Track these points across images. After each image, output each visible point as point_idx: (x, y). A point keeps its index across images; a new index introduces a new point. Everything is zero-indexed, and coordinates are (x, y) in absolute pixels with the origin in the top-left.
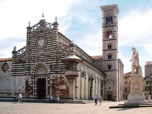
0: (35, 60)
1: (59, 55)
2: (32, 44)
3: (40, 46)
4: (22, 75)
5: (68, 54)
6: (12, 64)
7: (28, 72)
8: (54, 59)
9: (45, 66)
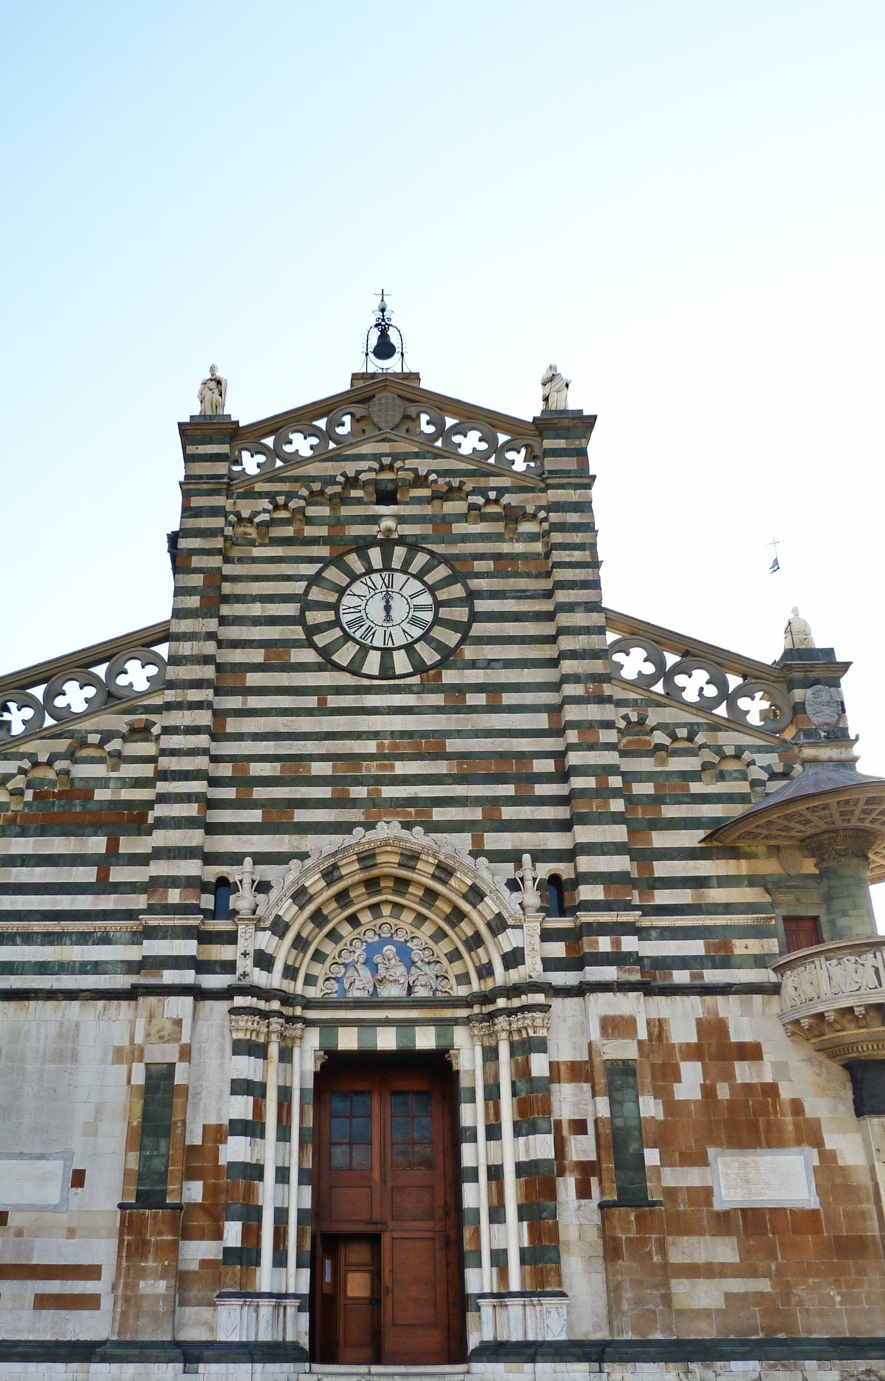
0: (303, 804)
2: (257, 609)
3: (364, 650)
7: (188, 947)
9: (461, 881)
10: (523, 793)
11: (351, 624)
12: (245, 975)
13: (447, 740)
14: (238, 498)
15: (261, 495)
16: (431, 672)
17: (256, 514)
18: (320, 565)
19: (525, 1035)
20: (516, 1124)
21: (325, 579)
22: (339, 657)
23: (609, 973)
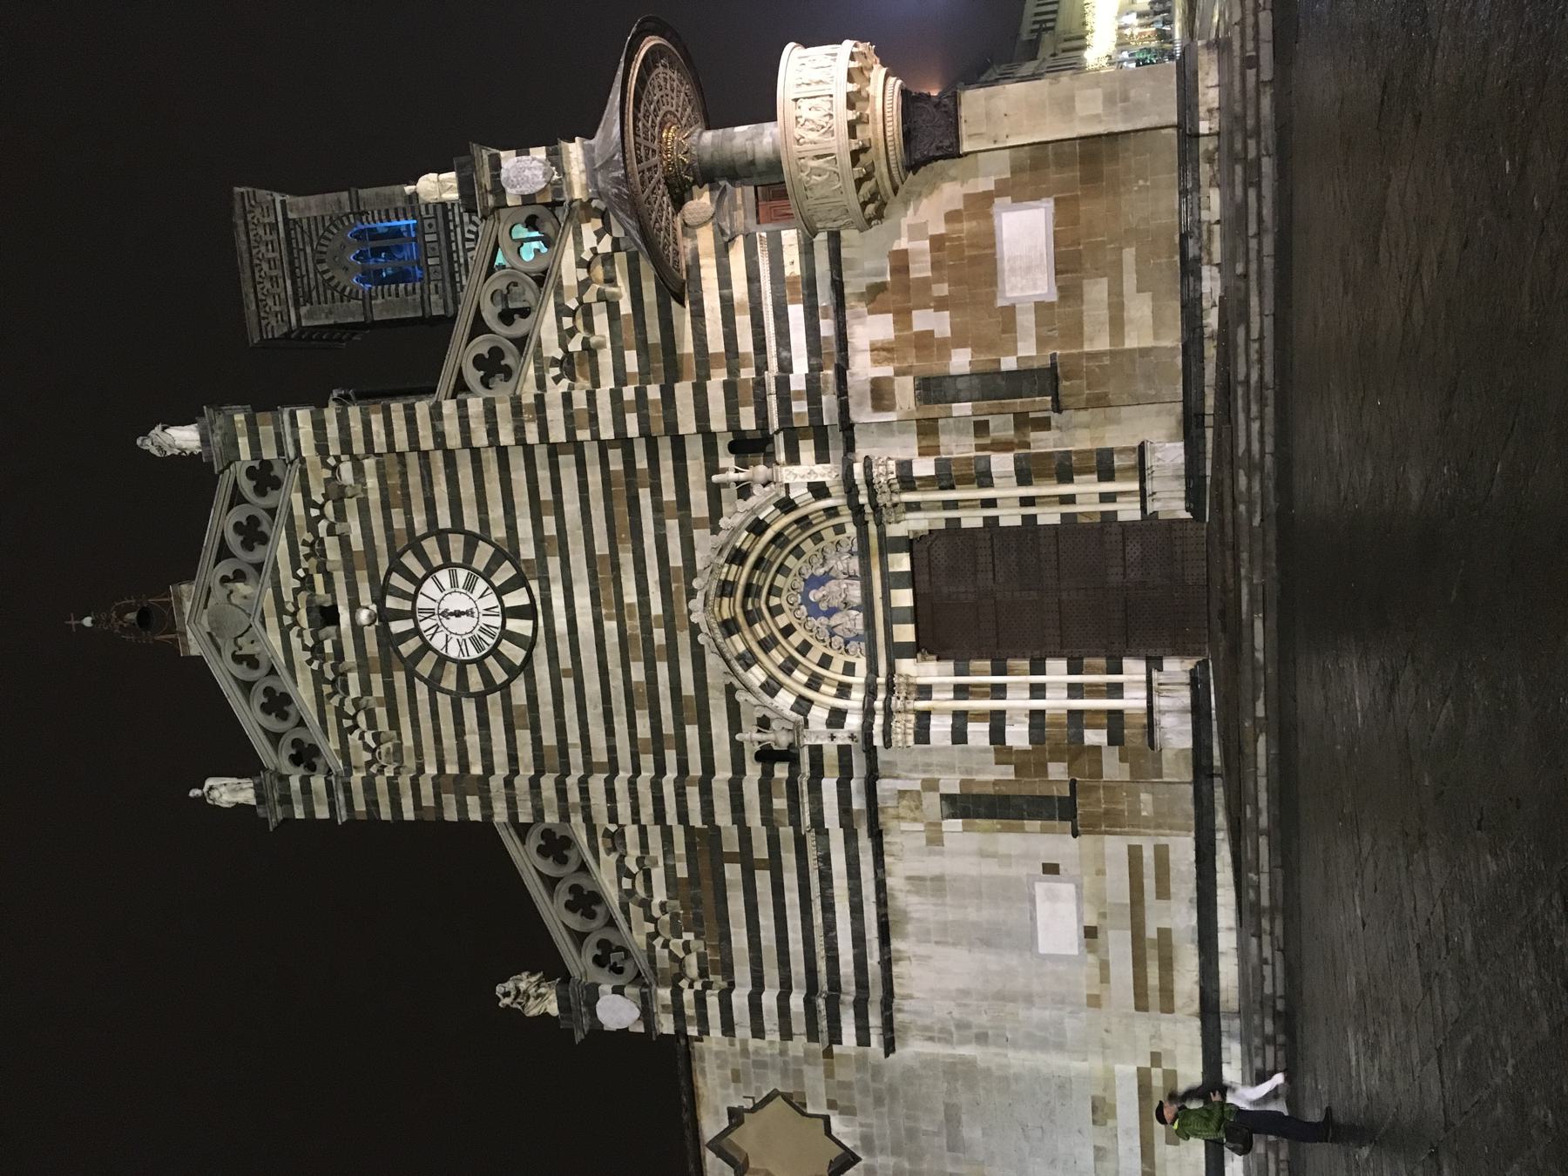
1: (605, 359)
2: (473, 740)
3: (506, 635)
4: (881, 886)
5: (588, 230)
6: (728, 1027)
7: (829, 785)
8: (656, 413)
9: (743, 539)
10: (648, 480)
11: (479, 648)
12: (852, 737)
13: (597, 553)
17: (367, 747)
18: (416, 680)
19: (896, 481)
20: (982, 486)
21: (431, 676)
22: (517, 658)
23: (829, 401)
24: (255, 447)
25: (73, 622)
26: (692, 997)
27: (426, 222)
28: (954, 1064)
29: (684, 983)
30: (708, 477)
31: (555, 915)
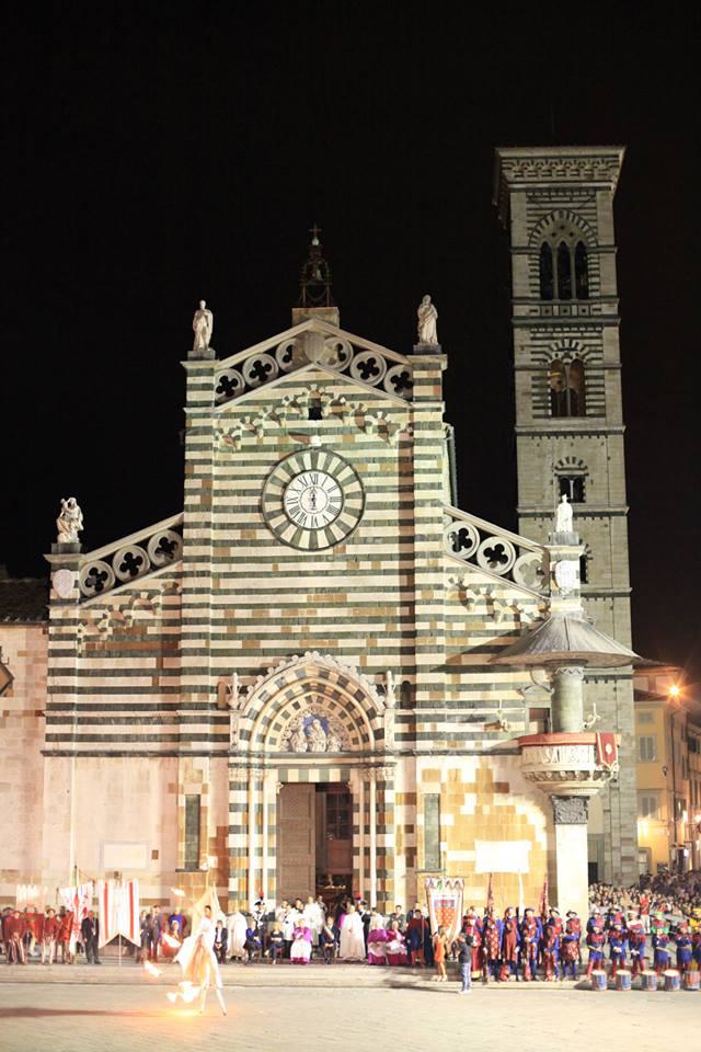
0: (264, 636)
2: (235, 501)
3: (301, 529)
4: (143, 754)
6: (55, 653)
7: (208, 729)
11: (291, 511)
12: (234, 744)
14: (222, 418)
15: (236, 415)
16: (340, 546)
17: (231, 431)
21: (275, 477)
24: (422, 382)
25: (315, 230)
26: (73, 632)
27: (586, 307)
28: (35, 789)
29: (80, 626)
30: (390, 668)
31: (125, 545)
